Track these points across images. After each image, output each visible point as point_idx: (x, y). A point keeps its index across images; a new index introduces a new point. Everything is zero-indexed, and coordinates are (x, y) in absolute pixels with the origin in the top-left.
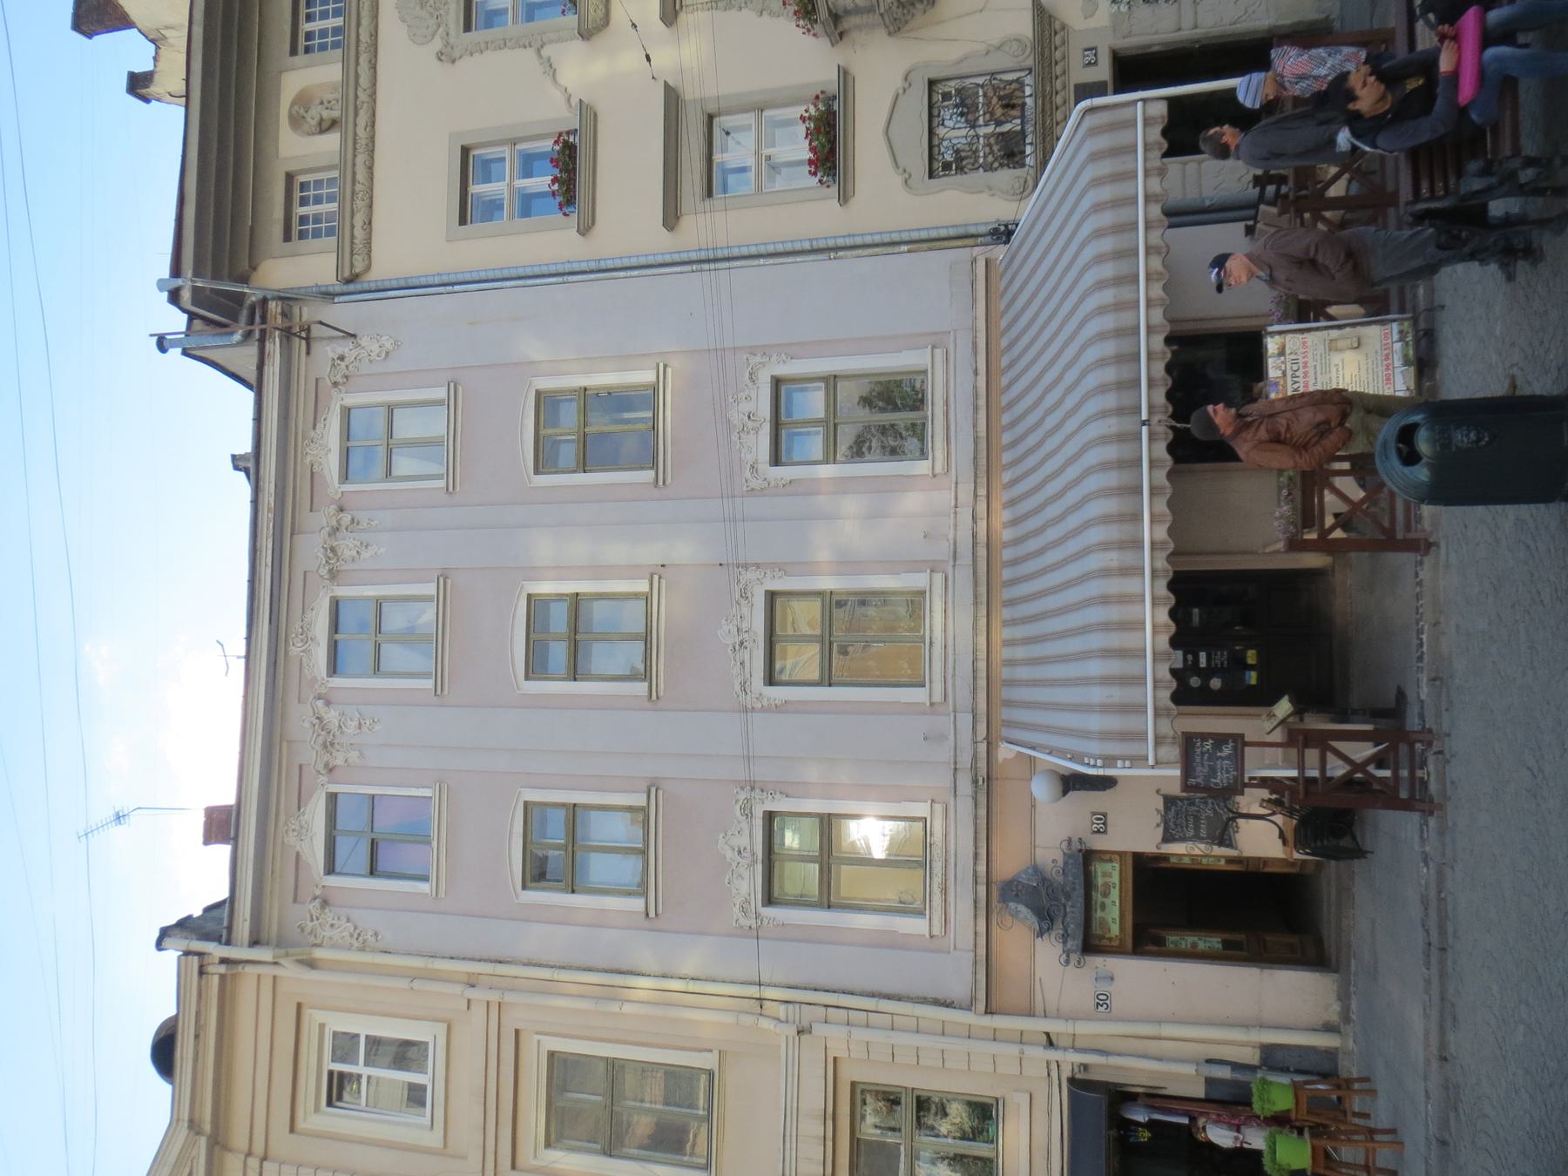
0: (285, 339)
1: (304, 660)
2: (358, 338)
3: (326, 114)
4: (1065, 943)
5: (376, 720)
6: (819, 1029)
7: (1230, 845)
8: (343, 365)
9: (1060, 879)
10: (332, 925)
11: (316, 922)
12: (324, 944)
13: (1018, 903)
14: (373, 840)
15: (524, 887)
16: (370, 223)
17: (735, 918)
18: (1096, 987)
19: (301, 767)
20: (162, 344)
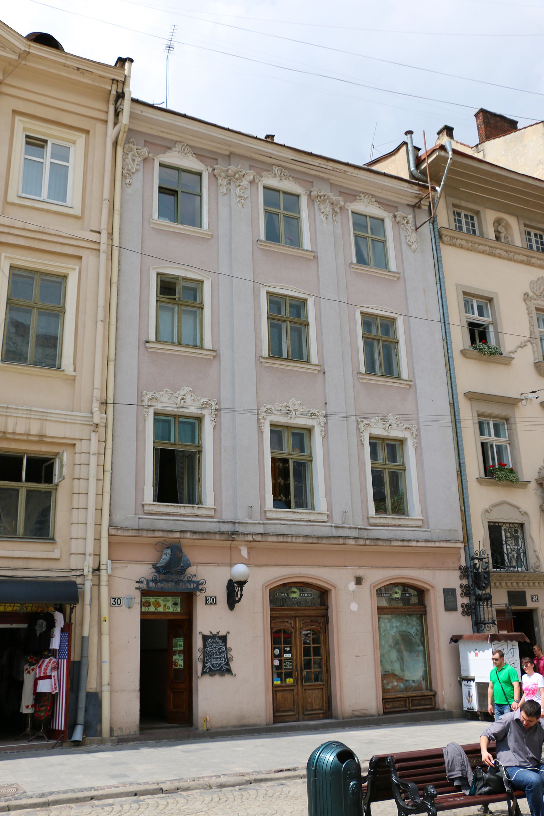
0: (417, 195)
1: (271, 173)
3: (502, 235)
4: (152, 581)
5: (244, 206)
6: (94, 437)
7: (203, 673)
8: (405, 222)
9: (186, 579)
11: (136, 150)
13: (171, 555)
14: (176, 192)
16: (462, 248)
17: (148, 393)
18: (124, 598)
20: (409, 133)
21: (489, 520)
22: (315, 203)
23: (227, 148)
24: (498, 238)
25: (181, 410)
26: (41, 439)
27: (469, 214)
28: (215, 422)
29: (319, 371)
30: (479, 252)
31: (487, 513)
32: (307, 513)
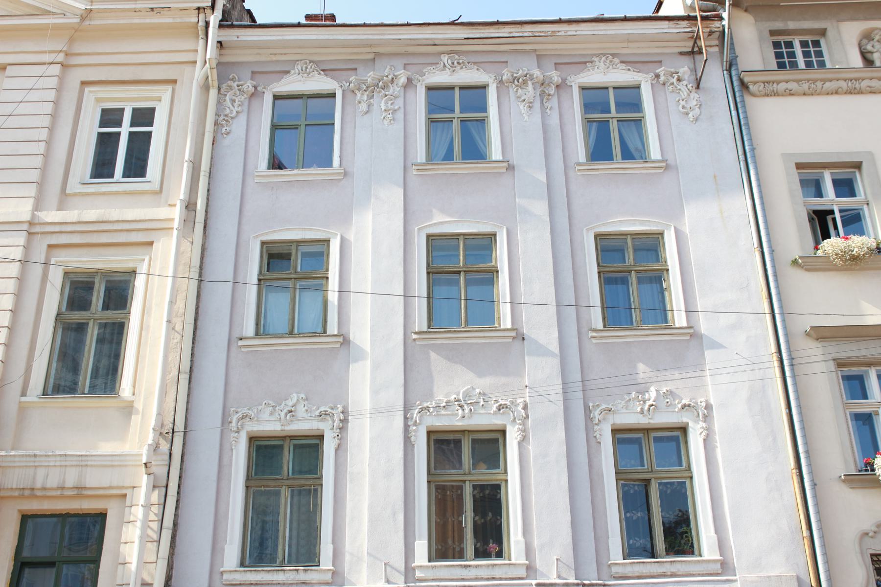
0: (690, 35)
1: (438, 66)
2: (697, 90)
8: (674, 80)
10: (234, 101)
11: (237, 88)
12: (220, 95)
15: (263, 243)
17: (239, 410)
19: (356, 69)
21: (873, 552)
22: (511, 89)
23: (368, 50)
24: (868, 62)
25: (287, 428)
26: (80, 491)
27: (809, 38)
28: (340, 439)
29: (514, 338)
30: (828, 94)
31: (867, 539)
32: (488, 566)
